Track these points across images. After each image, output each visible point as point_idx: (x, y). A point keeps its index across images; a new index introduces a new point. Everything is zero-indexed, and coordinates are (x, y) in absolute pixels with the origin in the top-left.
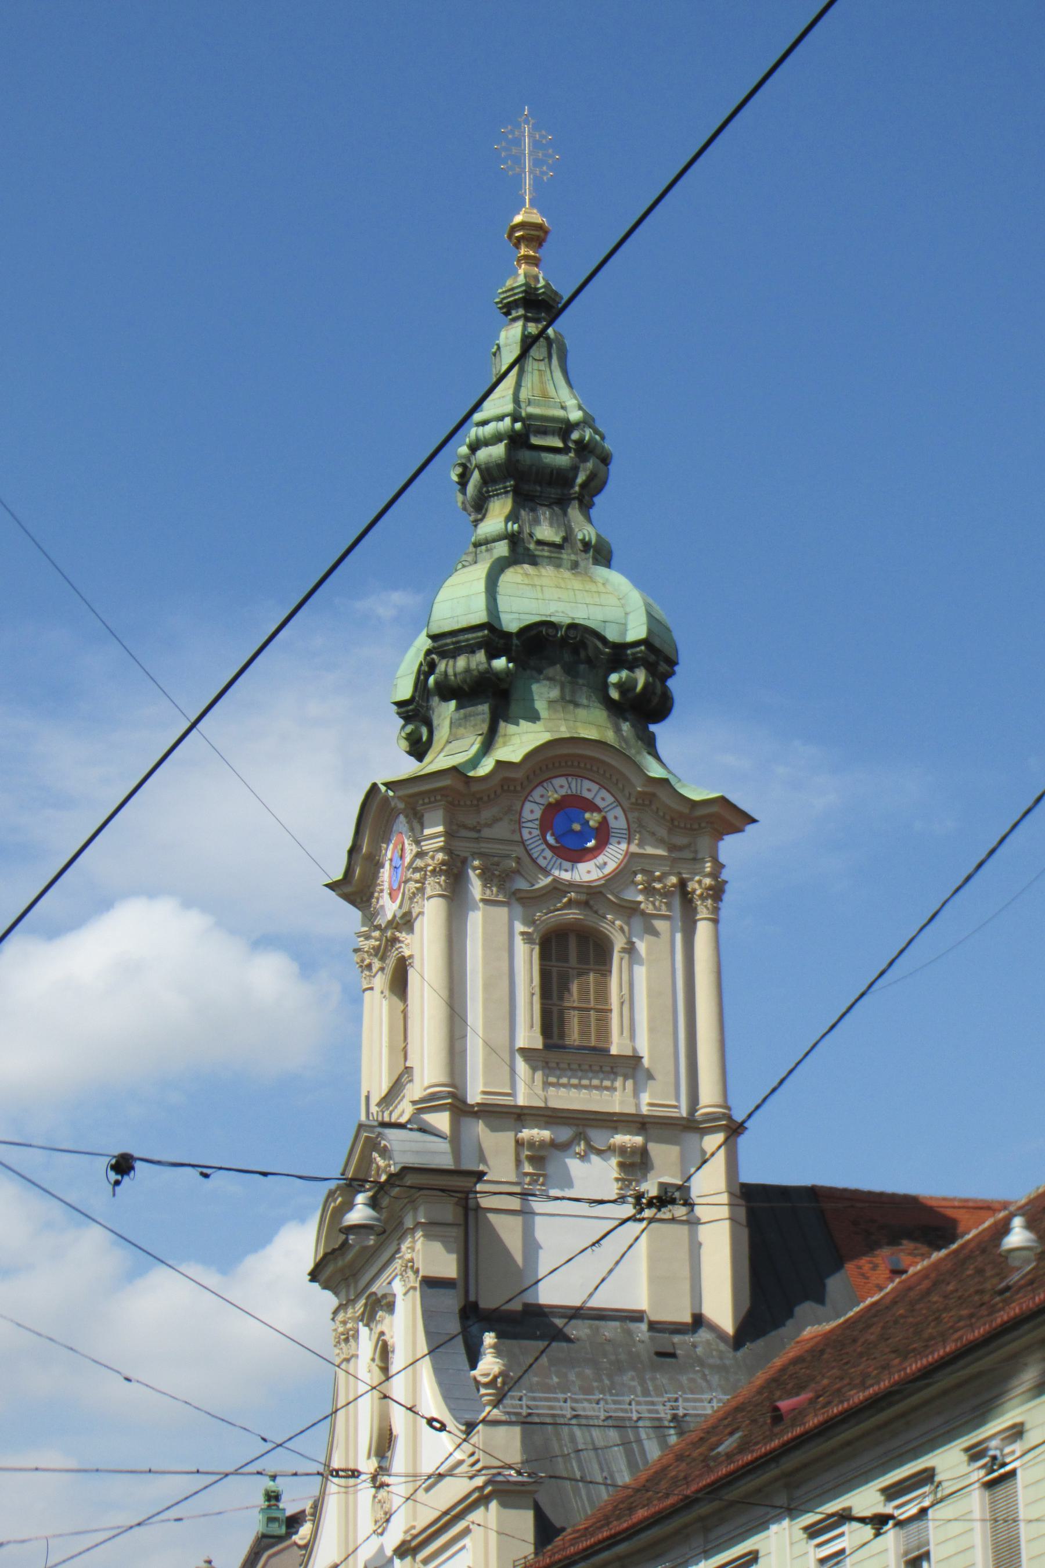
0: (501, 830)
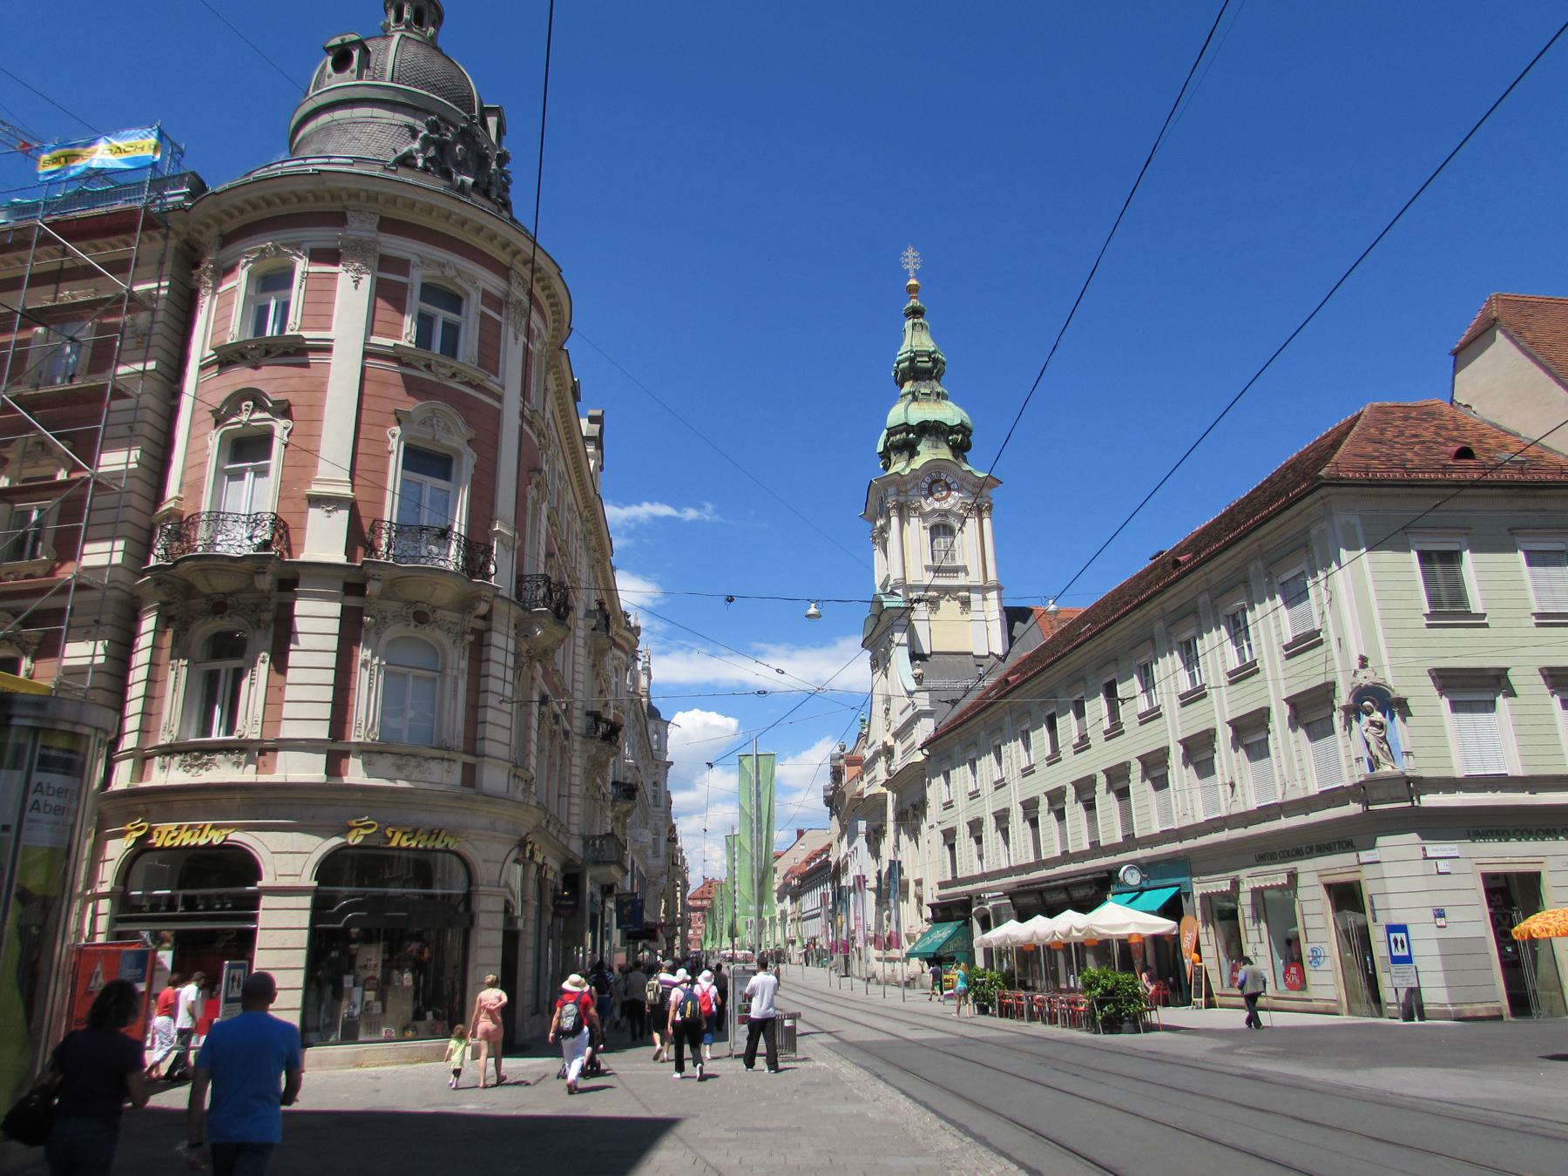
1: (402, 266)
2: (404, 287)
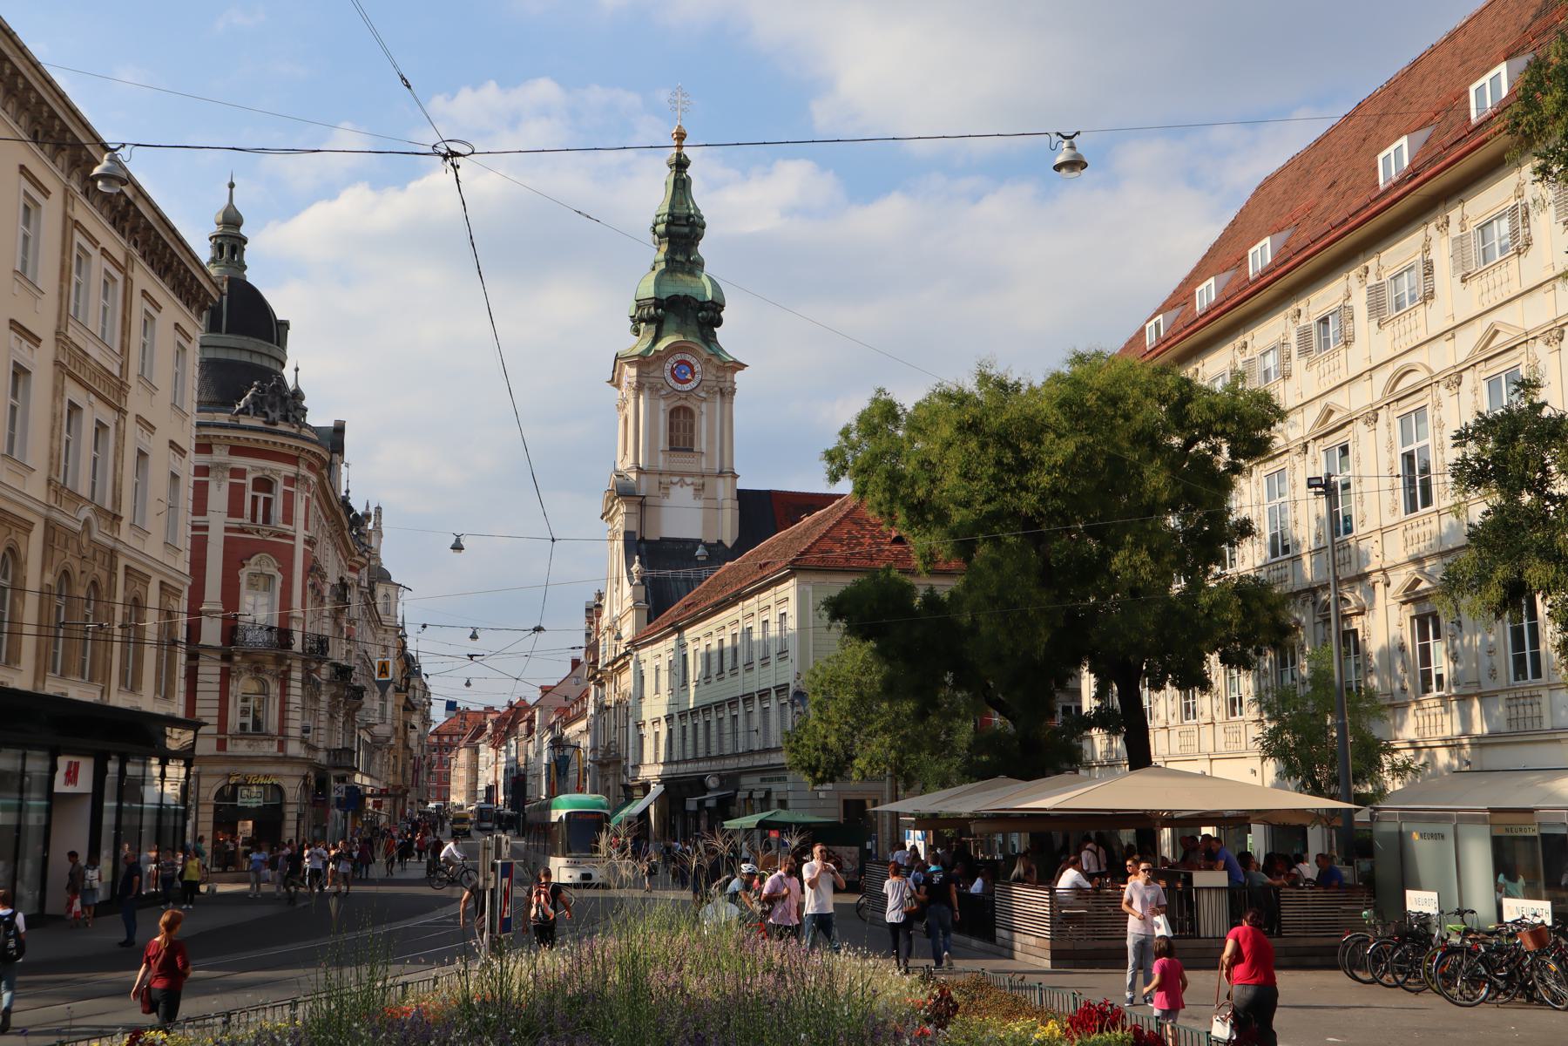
0: (657, 374)
1: (238, 473)
2: (243, 486)
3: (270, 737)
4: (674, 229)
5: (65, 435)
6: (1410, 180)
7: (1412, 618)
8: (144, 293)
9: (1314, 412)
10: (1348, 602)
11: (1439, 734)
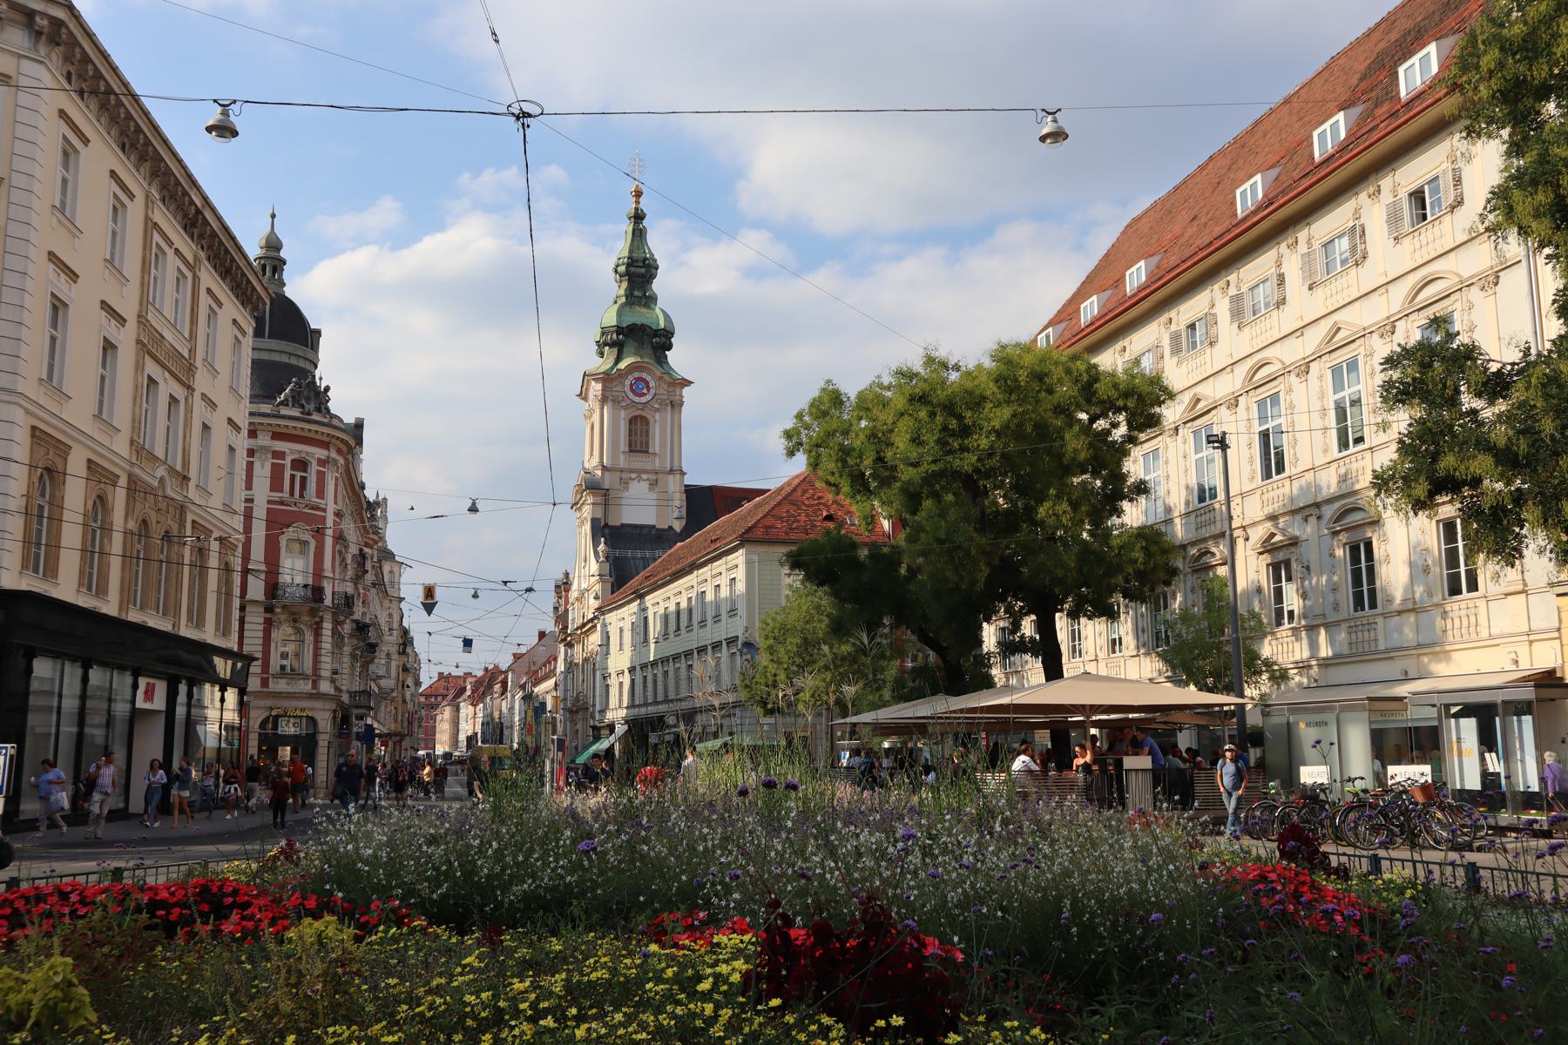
0: (618, 388)
1: (279, 455)
3: (304, 677)
4: (632, 269)
5: (145, 405)
6: (1267, 207)
7: (1268, 565)
8: (209, 290)
9: (1186, 398)
10: (1213, 554)
11: (1291, 659)
